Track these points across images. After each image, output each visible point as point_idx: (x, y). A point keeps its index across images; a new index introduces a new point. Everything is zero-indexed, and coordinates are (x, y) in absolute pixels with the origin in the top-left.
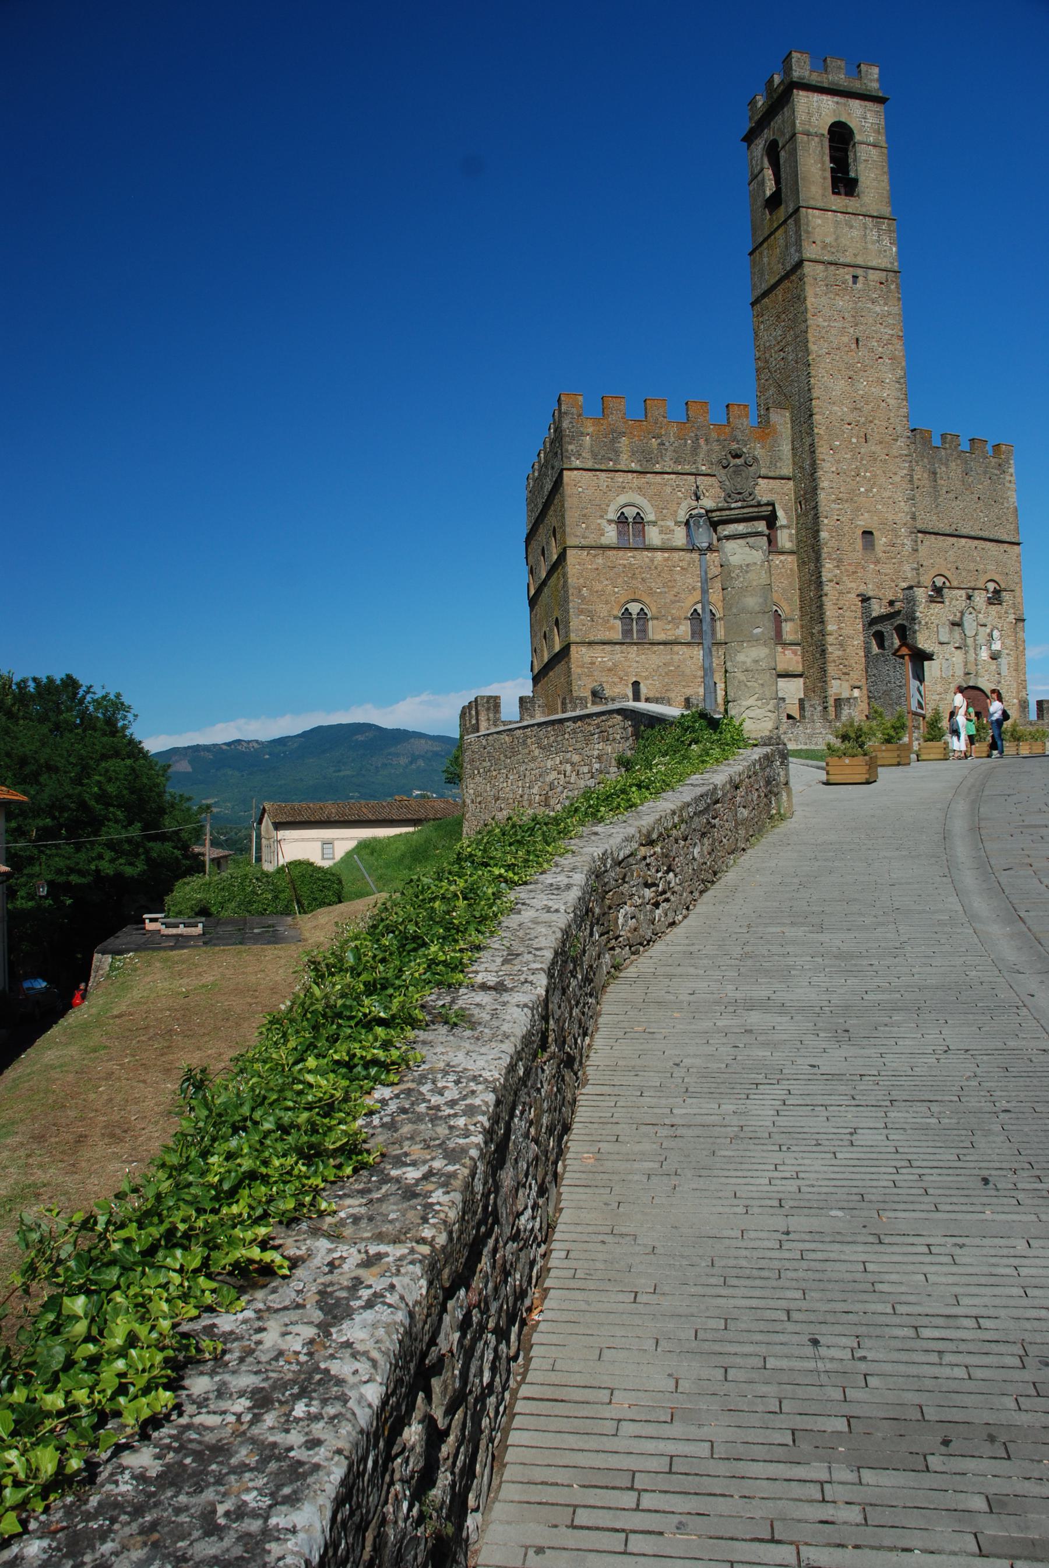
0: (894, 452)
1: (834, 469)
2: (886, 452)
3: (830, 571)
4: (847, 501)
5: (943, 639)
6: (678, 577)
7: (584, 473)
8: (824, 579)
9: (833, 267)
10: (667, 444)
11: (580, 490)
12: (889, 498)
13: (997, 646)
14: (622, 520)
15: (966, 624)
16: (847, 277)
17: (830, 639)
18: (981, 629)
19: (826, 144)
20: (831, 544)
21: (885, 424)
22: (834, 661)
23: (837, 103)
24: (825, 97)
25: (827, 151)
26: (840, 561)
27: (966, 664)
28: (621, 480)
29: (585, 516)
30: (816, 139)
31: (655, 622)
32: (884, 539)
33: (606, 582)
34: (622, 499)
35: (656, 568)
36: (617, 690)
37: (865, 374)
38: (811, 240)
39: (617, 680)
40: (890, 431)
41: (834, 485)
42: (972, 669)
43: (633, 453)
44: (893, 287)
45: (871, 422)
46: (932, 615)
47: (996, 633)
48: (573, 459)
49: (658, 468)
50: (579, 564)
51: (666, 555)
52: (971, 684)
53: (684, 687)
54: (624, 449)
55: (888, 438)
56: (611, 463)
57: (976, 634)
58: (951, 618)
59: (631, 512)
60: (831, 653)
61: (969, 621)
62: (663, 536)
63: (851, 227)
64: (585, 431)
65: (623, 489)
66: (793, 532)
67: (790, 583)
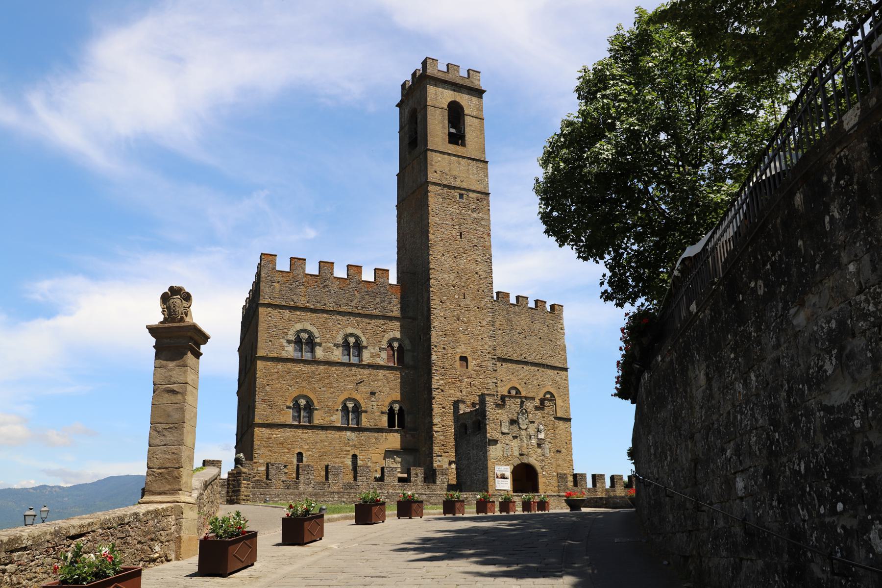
1: (442, 315)
5: (506, 431)
6: (333, 381)
10: (332, 291)
13: (542, 436)
14: (298, 342)
15: (520, 421)
17: (435, 428)
18: (530, 425)
19: (446, 113)
25: (447, 117)
27: (520, 447)
30: (440, 110)
34: (299, 326)
38: (434, 170)
39: (285, 450)
42: (525, 451)
59: (305, 336)
65: (299, 321)
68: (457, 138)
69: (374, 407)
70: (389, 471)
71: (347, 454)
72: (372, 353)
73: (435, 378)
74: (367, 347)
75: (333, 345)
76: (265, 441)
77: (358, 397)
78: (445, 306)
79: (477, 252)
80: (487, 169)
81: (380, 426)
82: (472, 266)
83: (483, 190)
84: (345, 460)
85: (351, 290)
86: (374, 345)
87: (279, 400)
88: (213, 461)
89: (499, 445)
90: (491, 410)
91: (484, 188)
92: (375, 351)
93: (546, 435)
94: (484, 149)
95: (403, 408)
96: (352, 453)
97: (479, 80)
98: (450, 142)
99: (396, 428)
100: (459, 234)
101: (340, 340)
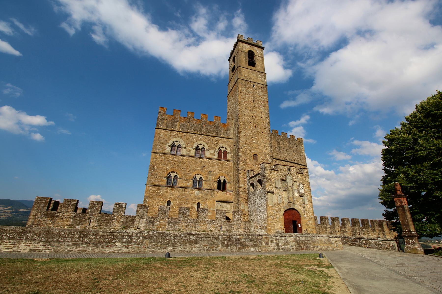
0: (265, 132)
1: (245, 135)
2: (262, 131)
3: (242, 166)
4: (249, 144)
5: (277, 186)
7: (163, 130)
8: (240, 168)
9: (247, 82)
10: (193, 125)
11: (160, 135)
13: (302, 191)
16: (251, 85)
18: (295, 183)
19: (247, 54)
20: (242, 157)
21: (262, 124)
24: (247, 45)
25: (247, 56)
26: (246, 163)
28: (175, 134)
29: (160, 143)
31: (180, 180)
32: (261, 158)
33: (164, 165)
34: (174, 139)
35: (183, 162)
36: (161, 204)
39: (161, 199)
40: (264, 126)
41: (244, 139)
43: (181, 126)
46: (272, 175)
47: (301, 186)
48: (160, 126)
49: (189, 131)
50: (155, 158)
51: (187, 158)
52: (291, 207)
53: (188, 204)
55: (263, 128)
56: (173, 128)
57: (292, 185)
58: (281, 177)
60: (241, 194)
61: (289, 179)
62: (187, 152)
63: (253, 73)
64: (166, 118)
66: (232, 155)
67: (230, 171)
68: (252, 63)
69: (211, 179)
70: (203, 211)
71: (195, 202)
72: (211, 153)
73: (241, 164)
77: (203, 173)
78: (246, 131)
80: (266, 76)
81: (213, 188)
82: (259, 114)
83: (264, 84)
85: (202, 125)
86: (212, 149)
87: (161, 173)
88: (70, 200)
89: (274, 196)
90: (268, 173)
93: (304, 190)
94: (264, 69)
96: (197, 202)
98: (248, 65)
99: (222, 190)
100: (253, 101)
101: (195, 146)
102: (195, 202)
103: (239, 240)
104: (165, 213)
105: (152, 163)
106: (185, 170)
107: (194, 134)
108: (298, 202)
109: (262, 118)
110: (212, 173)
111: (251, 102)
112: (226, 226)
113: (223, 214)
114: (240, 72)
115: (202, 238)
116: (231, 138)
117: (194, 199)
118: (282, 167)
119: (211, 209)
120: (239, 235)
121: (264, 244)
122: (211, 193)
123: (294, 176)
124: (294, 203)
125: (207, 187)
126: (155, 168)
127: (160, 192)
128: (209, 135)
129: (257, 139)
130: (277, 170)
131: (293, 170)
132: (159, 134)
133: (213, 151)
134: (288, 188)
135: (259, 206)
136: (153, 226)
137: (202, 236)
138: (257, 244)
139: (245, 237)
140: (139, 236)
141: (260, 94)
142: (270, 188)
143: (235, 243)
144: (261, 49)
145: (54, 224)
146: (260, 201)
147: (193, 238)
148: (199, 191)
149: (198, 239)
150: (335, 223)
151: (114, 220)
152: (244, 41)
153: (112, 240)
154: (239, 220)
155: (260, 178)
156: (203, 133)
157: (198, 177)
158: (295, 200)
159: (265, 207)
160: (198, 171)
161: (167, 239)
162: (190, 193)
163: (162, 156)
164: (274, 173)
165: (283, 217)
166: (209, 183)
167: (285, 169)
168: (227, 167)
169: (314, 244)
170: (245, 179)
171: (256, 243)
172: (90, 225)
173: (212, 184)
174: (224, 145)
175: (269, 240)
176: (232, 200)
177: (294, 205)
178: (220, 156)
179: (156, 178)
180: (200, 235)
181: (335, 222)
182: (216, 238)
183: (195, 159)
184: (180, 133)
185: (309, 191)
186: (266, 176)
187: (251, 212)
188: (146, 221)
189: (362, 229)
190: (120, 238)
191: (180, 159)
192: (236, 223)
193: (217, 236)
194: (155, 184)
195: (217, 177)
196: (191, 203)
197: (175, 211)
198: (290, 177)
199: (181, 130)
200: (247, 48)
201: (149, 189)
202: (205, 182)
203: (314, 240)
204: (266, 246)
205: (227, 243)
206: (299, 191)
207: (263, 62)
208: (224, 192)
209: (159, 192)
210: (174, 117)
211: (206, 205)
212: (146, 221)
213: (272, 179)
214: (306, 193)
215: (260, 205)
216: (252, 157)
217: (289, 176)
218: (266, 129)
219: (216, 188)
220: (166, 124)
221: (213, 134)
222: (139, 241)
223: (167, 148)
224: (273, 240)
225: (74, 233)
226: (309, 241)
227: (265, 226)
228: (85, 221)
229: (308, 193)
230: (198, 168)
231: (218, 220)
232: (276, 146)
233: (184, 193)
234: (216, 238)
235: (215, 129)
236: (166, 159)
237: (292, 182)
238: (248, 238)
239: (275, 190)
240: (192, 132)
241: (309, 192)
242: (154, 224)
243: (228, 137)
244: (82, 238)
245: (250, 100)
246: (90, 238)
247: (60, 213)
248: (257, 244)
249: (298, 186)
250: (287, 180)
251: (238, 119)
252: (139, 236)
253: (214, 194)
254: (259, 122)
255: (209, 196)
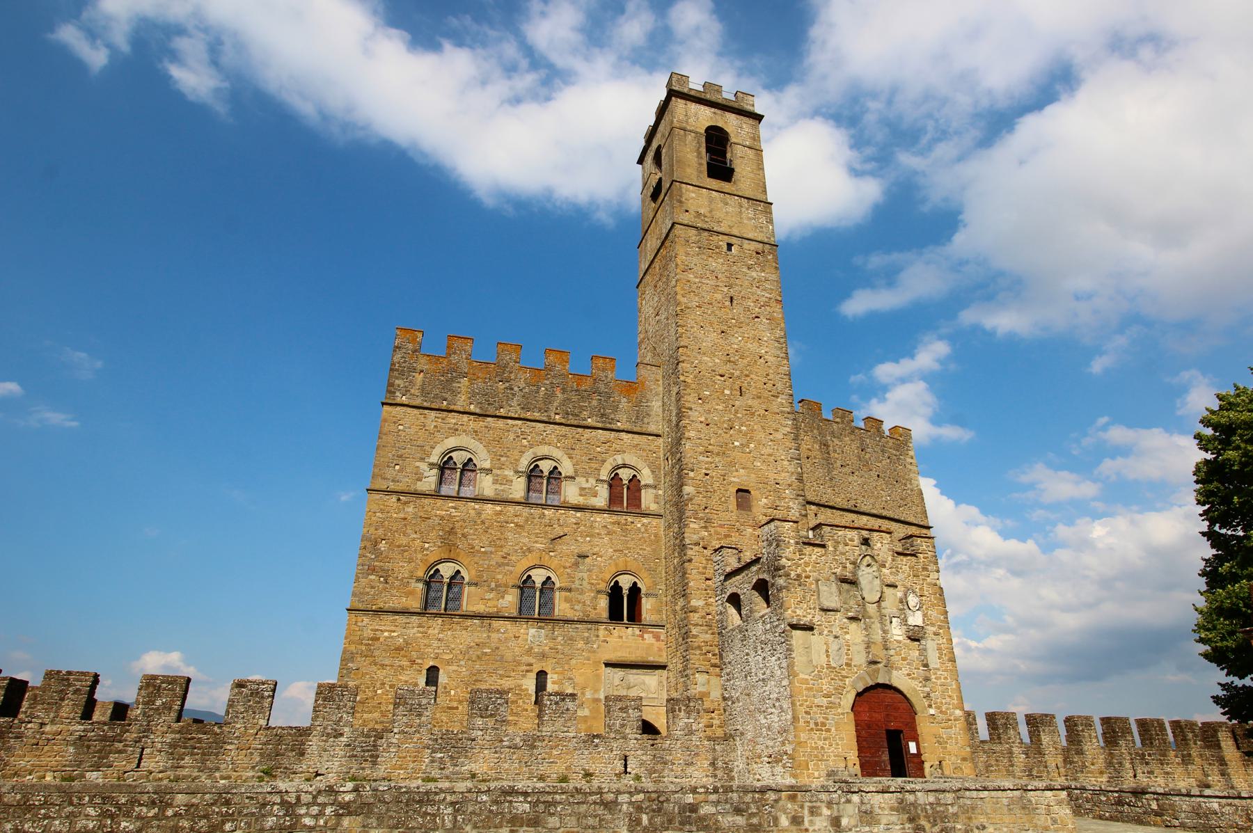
2: (764, 407)
3: (695, 532)
4: (718, 454)
5: (827, 604)
6: (510, 535)
7: (409, 410)
8: (687, 541)
9: (706, 234)
10: (516, 389)
11: (401, 427)
12: (770, 455)
13: (916, 619)
16: (721, 243)
18: (888, 591)
19: (703, 140)
20: (697, 500)
22: (699, 648)
23: (715, 113)
24: (702, 107)
26: (708, 521)
28: (454, 421)
31: (473, 588)
32: (764, 501)
33: (415, 536)
34: (451, 442)
35: (483, 522)
36: (403, 678)
37: (741, 330)
39: (405, 663)
40: (769, 386)
41: (702, 436)
43: (474, 394)
44: (769, 257)
45: (747, 376)
46: (807, 564)
47: (913, 600)
48: (398, 394)
49: (502, 412)
50: (382, 511)
51: (498, 508)
52: (881, 681)
53: (502, 677)
54: (463, 389)
55: (766, 394)
56: (445, 403)
58: (838, 571)
61: (866, 576)
62: (498, 486)
63: (727, 204)
65: (455, 431)
66: (661, 492)
67: (654, 550)
68: (720, 169)
69: (585, 583)
70: (557, 703)
71: (527, 671)
72: (582, 489)
73: (692, 525)
74: (574, 478)
75: (512, 473)
76: (366, 645)
77: (554, 563)
78: (707, 407)
79: (761, 327)
81: (593, 616)
82: (752, 346)
83: (766, 240)
84: (521, 682)
86: (587, 475)
88: (69, 673)
89: (815, 639)
90: (790, 556)
91: (767, 238)
92: (585, 485)
93: (925, 615)
94: (765, 188)
95: (639, 585)
97: (753, 105)
98: (710, 176)
99: (625, 621)
101: (524, 463)
102: (527, 671)
103: (693, 808)
104: (420, 715)
105: (372, 530)
106: (491, 553)
107: (520, 422)
108: (904, 659)
109: (762, 360)
110: (587, 560)
111: (720, 305)
112: (644, 758)
113: (630, 711)
114: (681, 202)
115: (555, 803)
116: (656, 432)
117: (526, 659)
118: (840, 533)
119: (588, 695)
120: (694, 790)
121: (784, 821)
122: (586, 634)
123: (884, 566)
124: (889, 666)
125: (570, 615)
126: (383, 546)
127: (398, 636)
128: (575, 423)
129: (745, 434)
130: (823, 546)
131: (879, 545)
132: (394, 422)
133: (592, 481)
134: (865, 610)
135: (763, 679)
136: (374, 763)
137: (557, 797)
138: (760, 824)
139: (713, 797)
140: (324, 805)
141: (751, 277)
142: (798, 612)
143: (678, 819)
144: (751, 121)
145: (6, 765)
146: (764, 658)
147: (522, 807)
148: (540, 628)
149: (541, 807)
150: (1043, 737)
151: (231, 743)
152: (692, 93)
153: (223, 823)
154: (691, 733)
155: (761, 577)
156: (552, 415)
157: (538, 577)
158: (892, 652)
159: (785, 683)
160: (538, 555)
161: (426, 814)
162: (512, 635)
163: (406, 503)
164: (814, 557)
165: (852, 715)
166: (581, 597)
167: (852, 540)
168: (643, 537)
169: (970, 818)
170: (707, 579)
171: (755, 821)
172: (138, 766)
173: (588, 602)
174: (630, 459)
175: (802, 807)
176: (662, 660)
177: (889, 672)
178: (614, 498)
179: (387, 583)
180: (549, 793)
181: (1044, 730)
182: (606, 805)
183: (527, 509)
184: (472, 417)
185: (942, 617)
186: (784, 567)
187: (733, 703)
188: (349, 745)
189: (1143, 755)
190: (253, 814)
191: (472, 512)
192: (679, 745)
193: (611, 797)
194: (382, 605)
195: (608, 576)
196: (513, 674)
197: (455, 704)
198: (869, 570)
199: (475, 407)
200: (704, 117)
201: (359, 624)
202: (564, 593)
203: (968, 802)
204: (793, 828)
205: (650, 820)
206: (904, 621)
207: (759, 164)
208: (634, 630)
209: (395, 634)
210: (450, 363)
211: (570, 679)
212: (349, 745)
213: (806, 577)
214: (933, 625)
215: (764, 674)
216: (733, 500)
217: (868, 565)
218: (777, 397)
219: (605, 615)
220: (422, 389)
221: (589, 420)
222: (322, 822)
223: (426, 474)
224: (819, 804)
225: (80, 799)
226: (952, 805)
227: (786, 753)
228: (120, 752)
229: (940, 627)
230: (536, 542)
231: (612, 735)
232: (815, 458)
233: (489, 637)
234: (606, 805)
235: (595, 403)
236: (422, 514)
237: (879, 589)
238: (726, 802)
239: (818, 618)
240: (513, 415)
241: (942, 621)
242: (378, 756)
243: (644, 430)
244: (112, 816)
245: (719, 296)
246: (139, 817)
247: (29, 726)
248: (760, 824)
249: (901, 602)
250: (861, 579)
251: (677, 364)
252: (324, 805)
253: (598, 636)
254: (751, 372)
255: (581, 644)
